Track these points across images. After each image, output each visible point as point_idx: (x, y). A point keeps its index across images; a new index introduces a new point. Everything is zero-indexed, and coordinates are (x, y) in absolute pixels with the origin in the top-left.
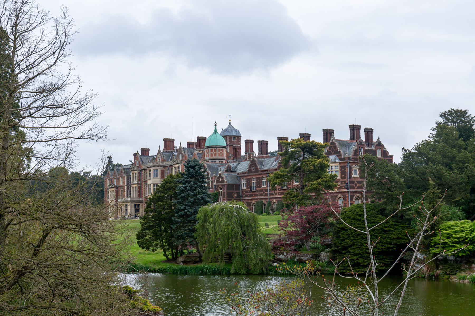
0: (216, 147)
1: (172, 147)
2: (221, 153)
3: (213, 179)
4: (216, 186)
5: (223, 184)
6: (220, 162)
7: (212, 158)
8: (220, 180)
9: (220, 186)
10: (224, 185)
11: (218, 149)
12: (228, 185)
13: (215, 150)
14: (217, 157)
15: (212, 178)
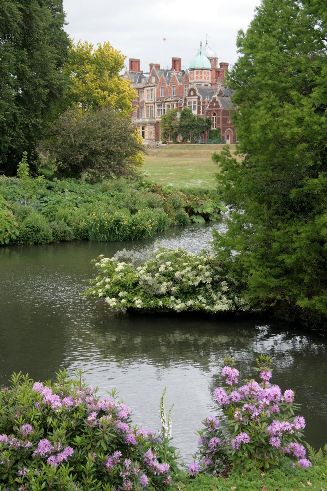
0: (202, 69)
1: (137, 68)
2: (207, 76)
3: (205, 104)
4: (209, 111)
5: (218, 109)
6: (205, 85)
7: (197, 81)
8: (214, 104)
9: (214, 112)
10: (219, 110)
11: (204, 71)
12: (224, 111)
13: (201, 73)
14: (203, 80)
15: (203, 103)
